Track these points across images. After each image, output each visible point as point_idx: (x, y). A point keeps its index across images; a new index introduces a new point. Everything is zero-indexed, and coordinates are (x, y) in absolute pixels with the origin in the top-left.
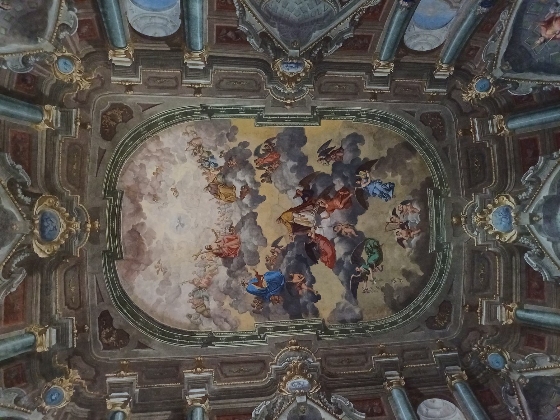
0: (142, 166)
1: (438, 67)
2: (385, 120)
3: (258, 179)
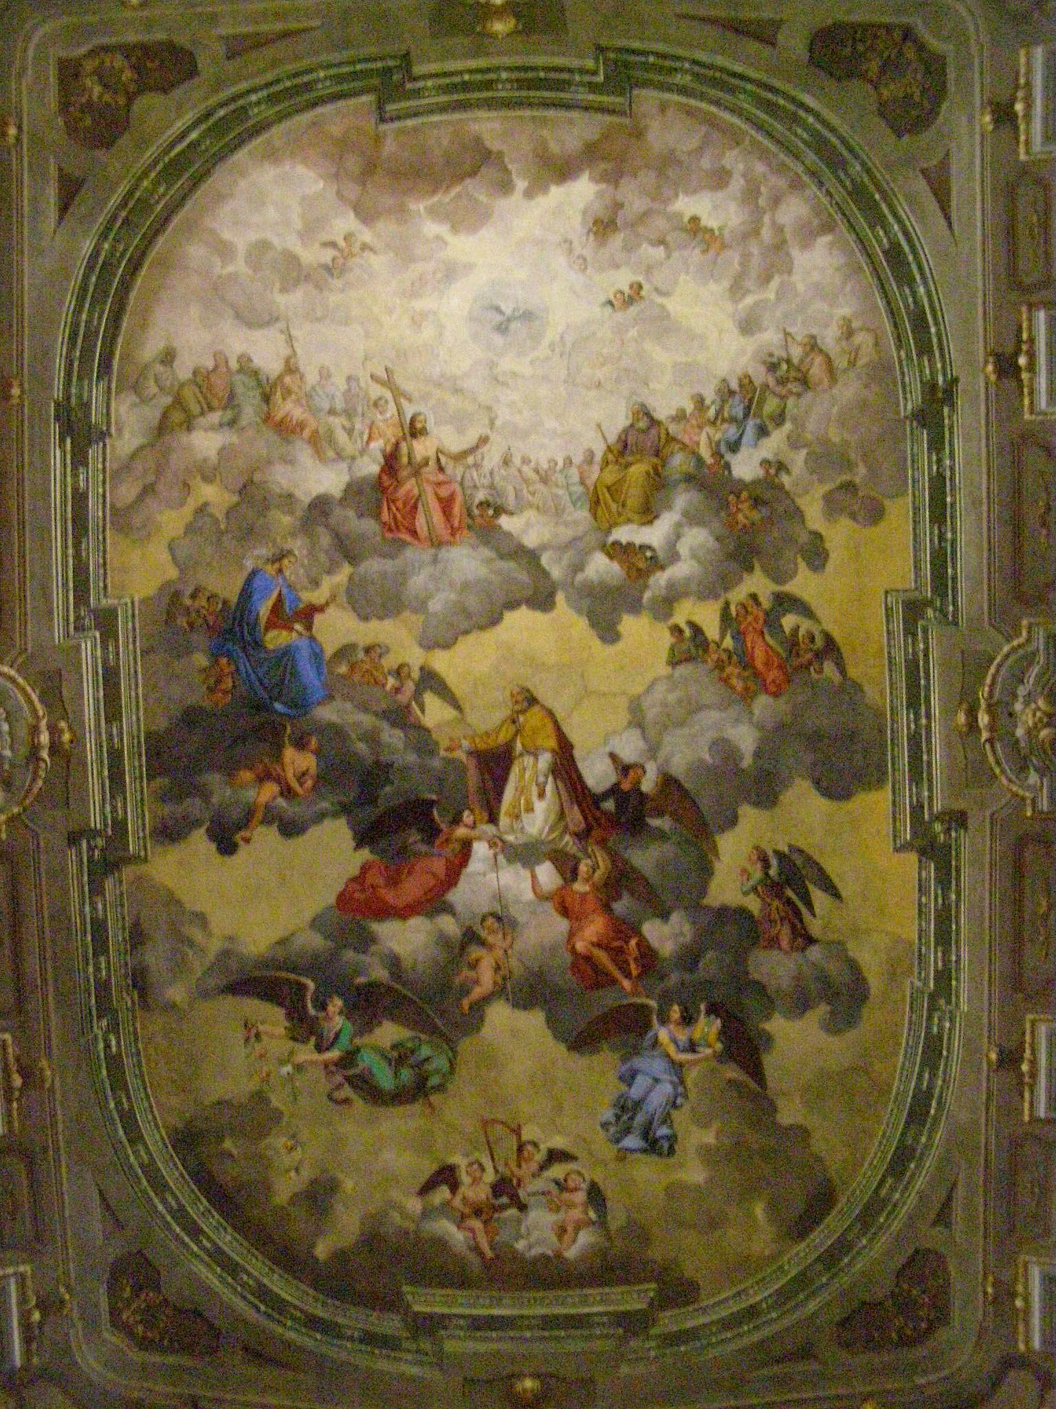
0: (720, 179)
2: (918, 1114)
3: (683, 613)
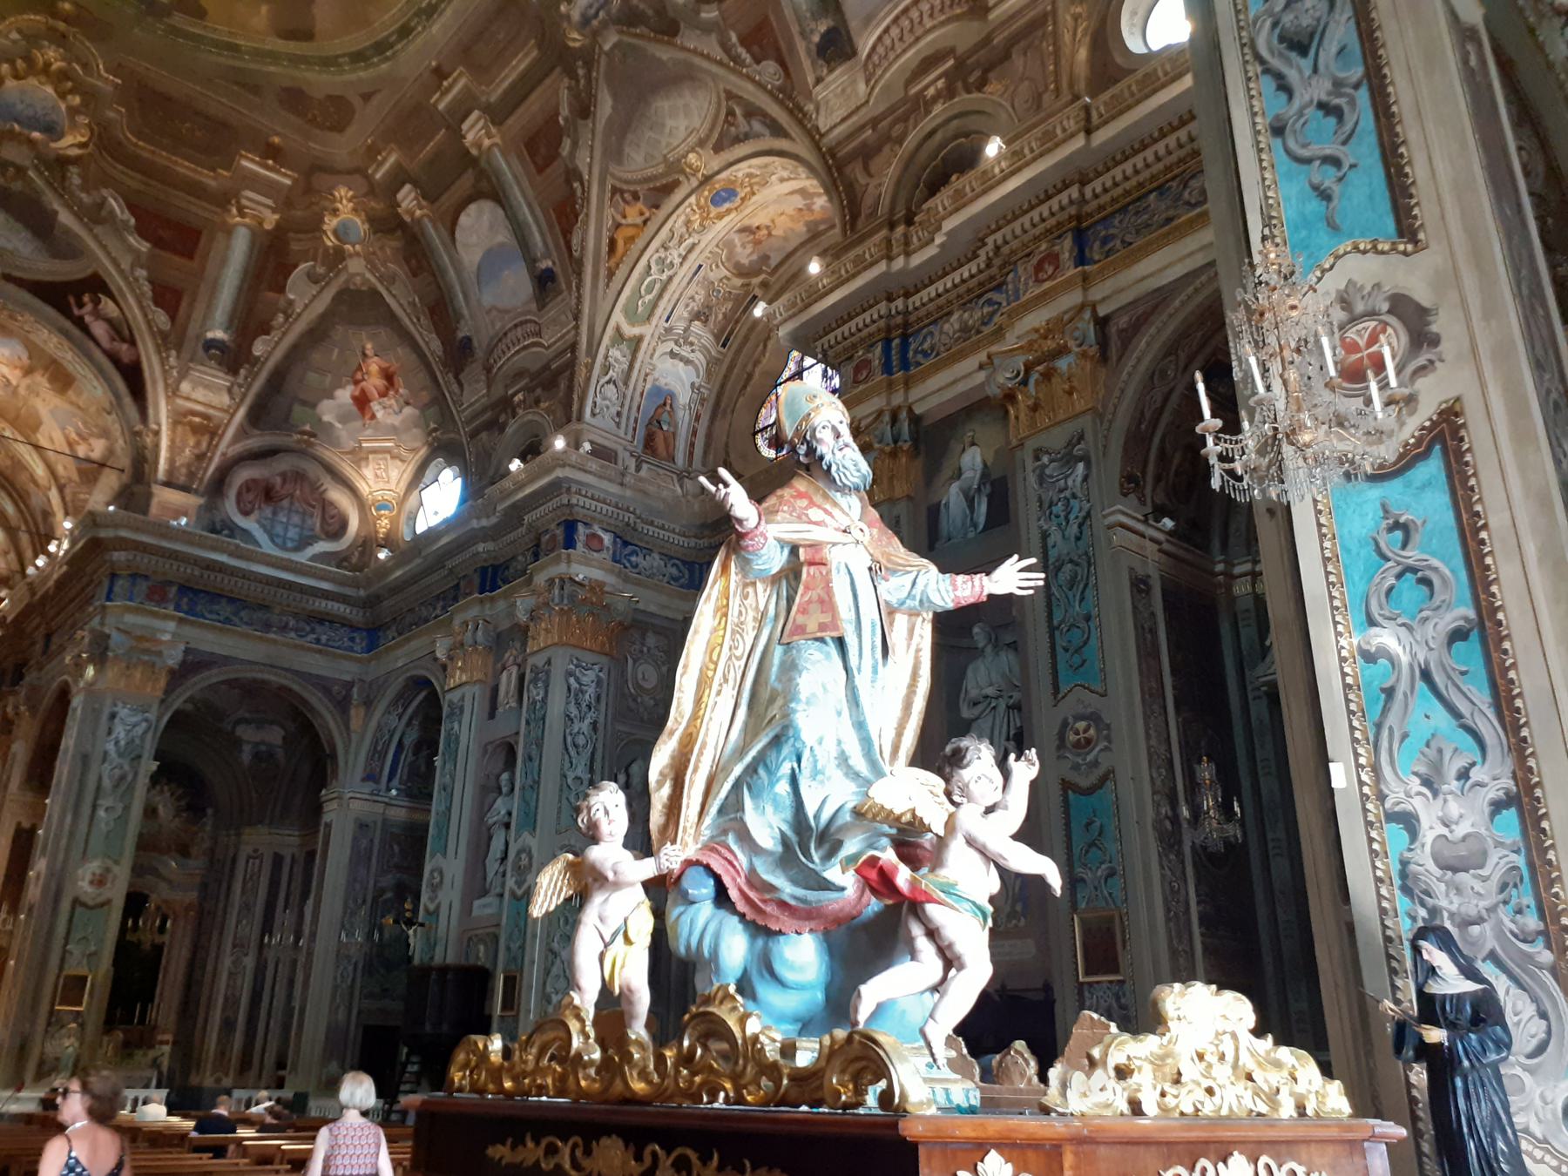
1: (424, 203)
2: (381, 48)
